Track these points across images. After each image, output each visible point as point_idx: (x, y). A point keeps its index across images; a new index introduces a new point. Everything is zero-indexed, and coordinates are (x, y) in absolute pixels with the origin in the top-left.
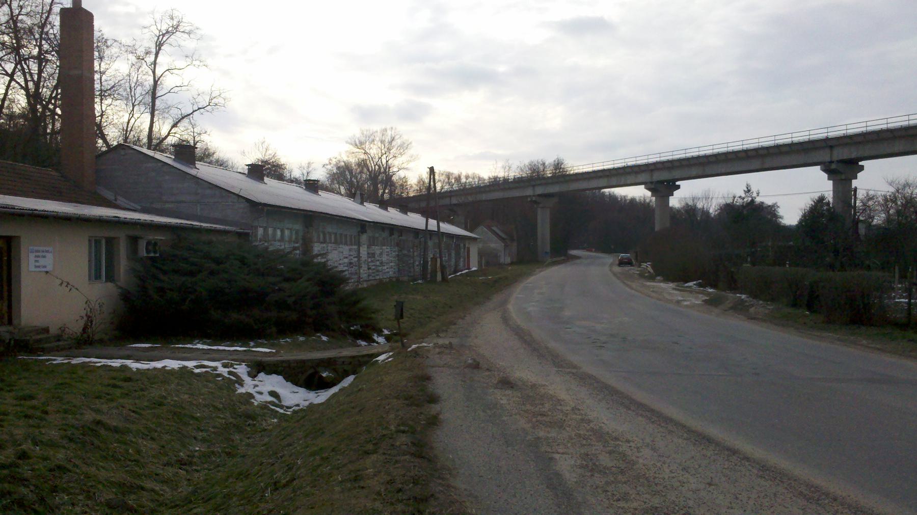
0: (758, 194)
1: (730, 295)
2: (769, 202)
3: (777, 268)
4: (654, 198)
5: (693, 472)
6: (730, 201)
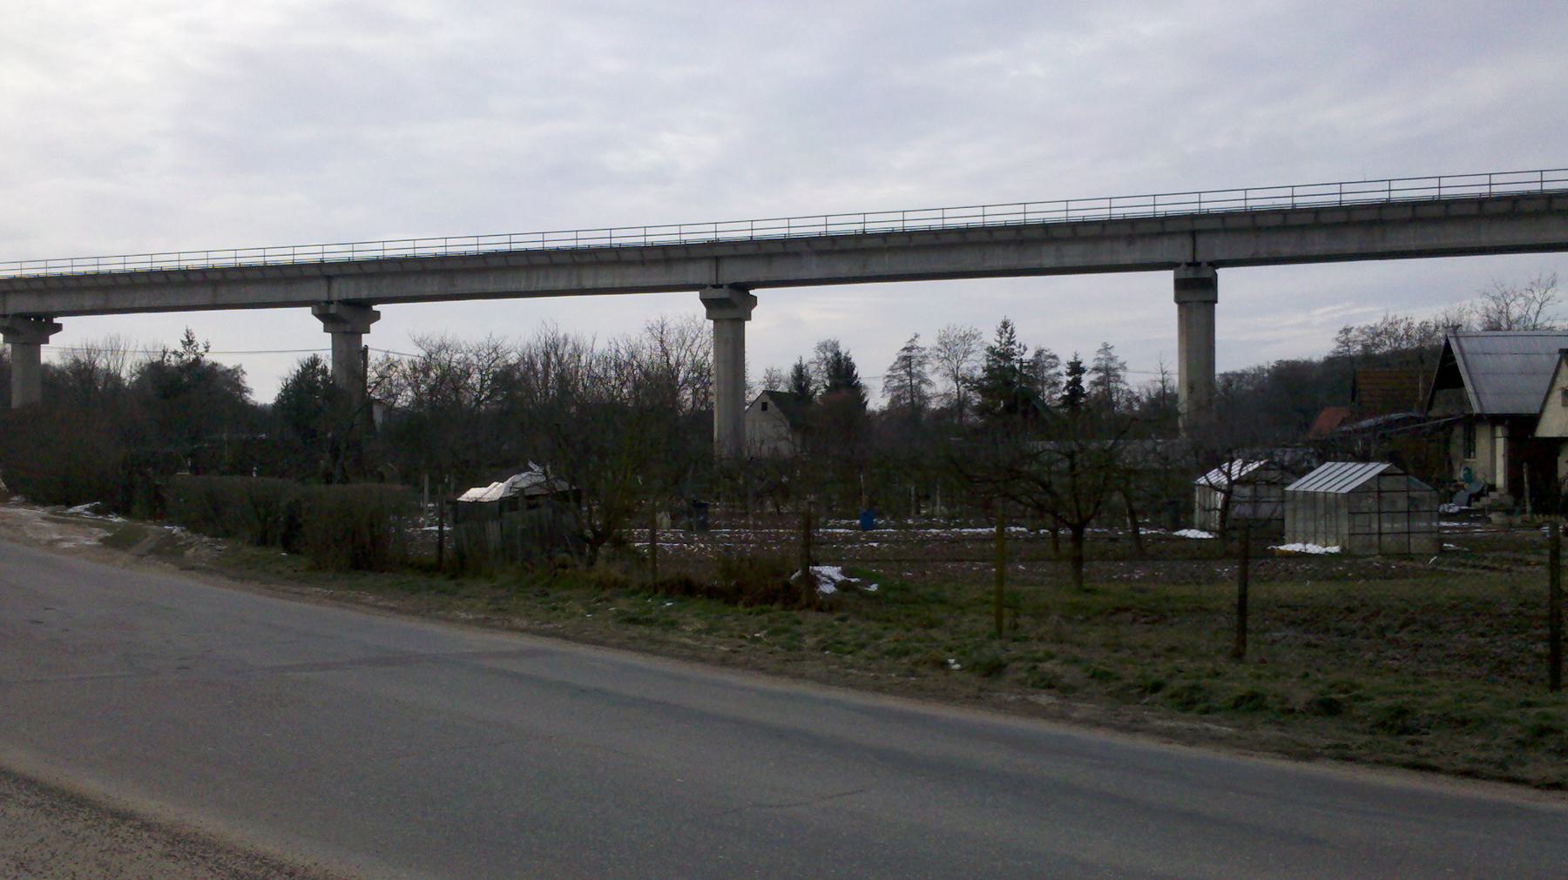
0: (207, 348)
1: (152, 528)
2: (227, 362)
3: (237, 479)
4: (9, 346)
5: (39, 868)
6: (157, 358)
